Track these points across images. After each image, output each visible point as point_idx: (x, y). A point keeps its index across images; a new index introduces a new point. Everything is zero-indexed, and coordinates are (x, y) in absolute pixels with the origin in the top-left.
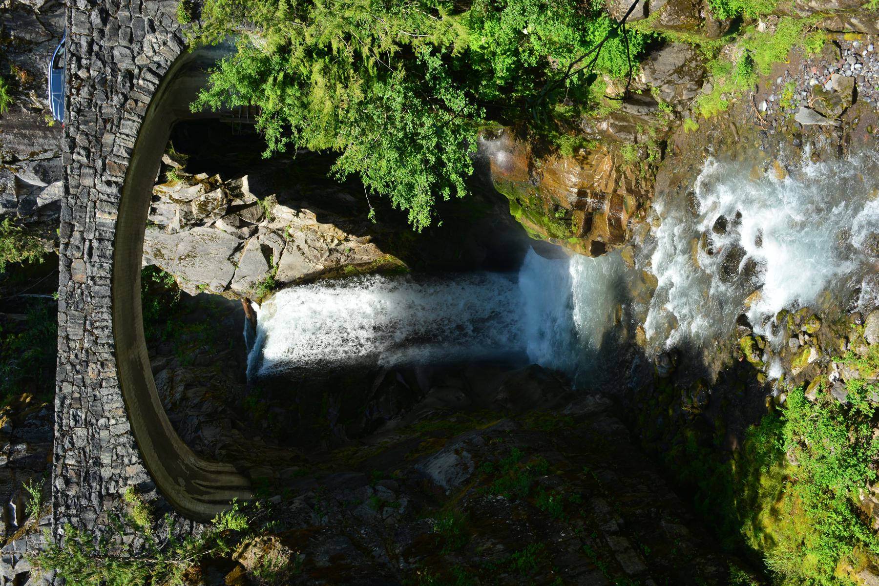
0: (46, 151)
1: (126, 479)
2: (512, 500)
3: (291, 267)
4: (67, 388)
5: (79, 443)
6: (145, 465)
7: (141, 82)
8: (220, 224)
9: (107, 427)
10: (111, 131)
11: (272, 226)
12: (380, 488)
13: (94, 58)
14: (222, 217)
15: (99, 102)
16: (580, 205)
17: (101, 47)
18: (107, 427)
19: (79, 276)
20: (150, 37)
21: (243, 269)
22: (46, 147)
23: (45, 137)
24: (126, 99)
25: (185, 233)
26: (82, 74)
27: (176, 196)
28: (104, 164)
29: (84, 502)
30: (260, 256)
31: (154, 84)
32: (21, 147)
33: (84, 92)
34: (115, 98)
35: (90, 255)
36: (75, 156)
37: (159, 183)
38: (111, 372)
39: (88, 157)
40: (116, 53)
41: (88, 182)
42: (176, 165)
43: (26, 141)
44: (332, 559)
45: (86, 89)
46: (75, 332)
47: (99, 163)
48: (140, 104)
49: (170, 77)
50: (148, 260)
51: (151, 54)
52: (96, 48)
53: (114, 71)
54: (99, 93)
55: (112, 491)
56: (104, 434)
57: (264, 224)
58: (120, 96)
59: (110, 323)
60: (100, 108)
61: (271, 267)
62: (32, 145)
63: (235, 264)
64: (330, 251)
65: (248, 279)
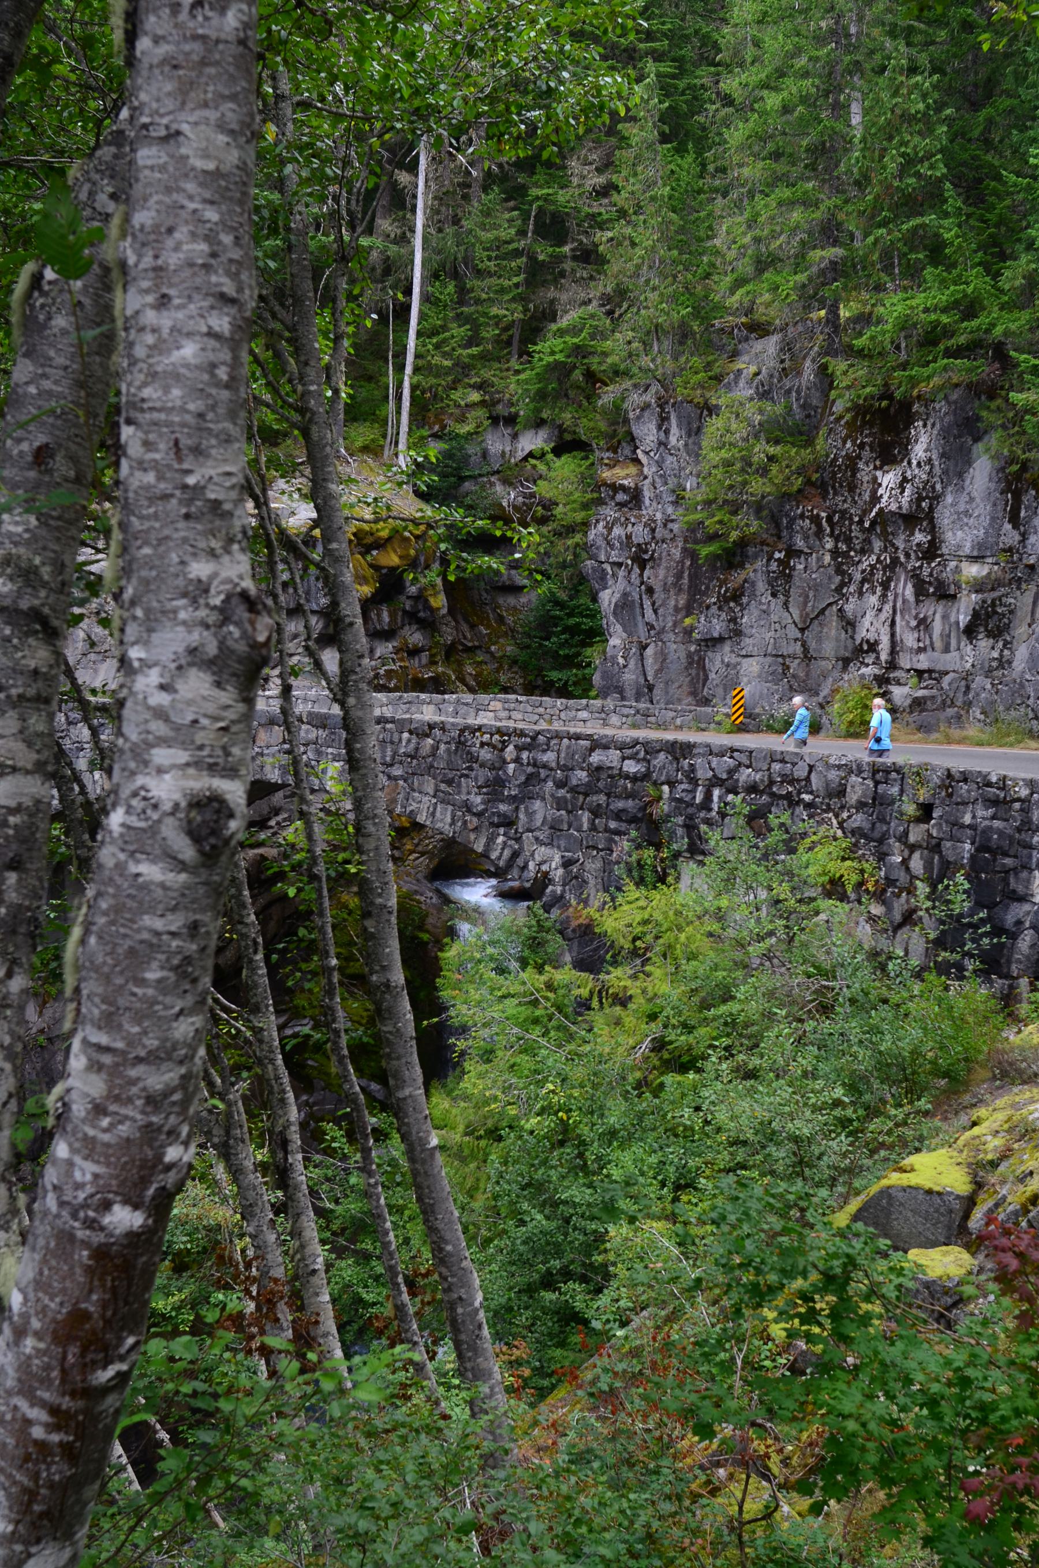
0: (655, 611)
7: (500, 839)
10: (437, 791)
13: (530, 770)
15: (473, 774)
17: (545, 781)
20: (557, 860)
22: (661, 611)
24: (479, 815)
26: (510, 752)
28: (396, 779)
31: (499, 858)
32: (662, 572)
34: (478, 799)
36: (406, 735)
39: (407, 755)
40: (537, 805)
43: (670, 580)
45: (489, 756)
47: (397, 771)
48: (472, 836)
51: (538, 858)
52: (543, 773)
53: (513, 799)
54: (483, 775)
58: (481, 808)
60: (467, 776)
62: (666, 589)
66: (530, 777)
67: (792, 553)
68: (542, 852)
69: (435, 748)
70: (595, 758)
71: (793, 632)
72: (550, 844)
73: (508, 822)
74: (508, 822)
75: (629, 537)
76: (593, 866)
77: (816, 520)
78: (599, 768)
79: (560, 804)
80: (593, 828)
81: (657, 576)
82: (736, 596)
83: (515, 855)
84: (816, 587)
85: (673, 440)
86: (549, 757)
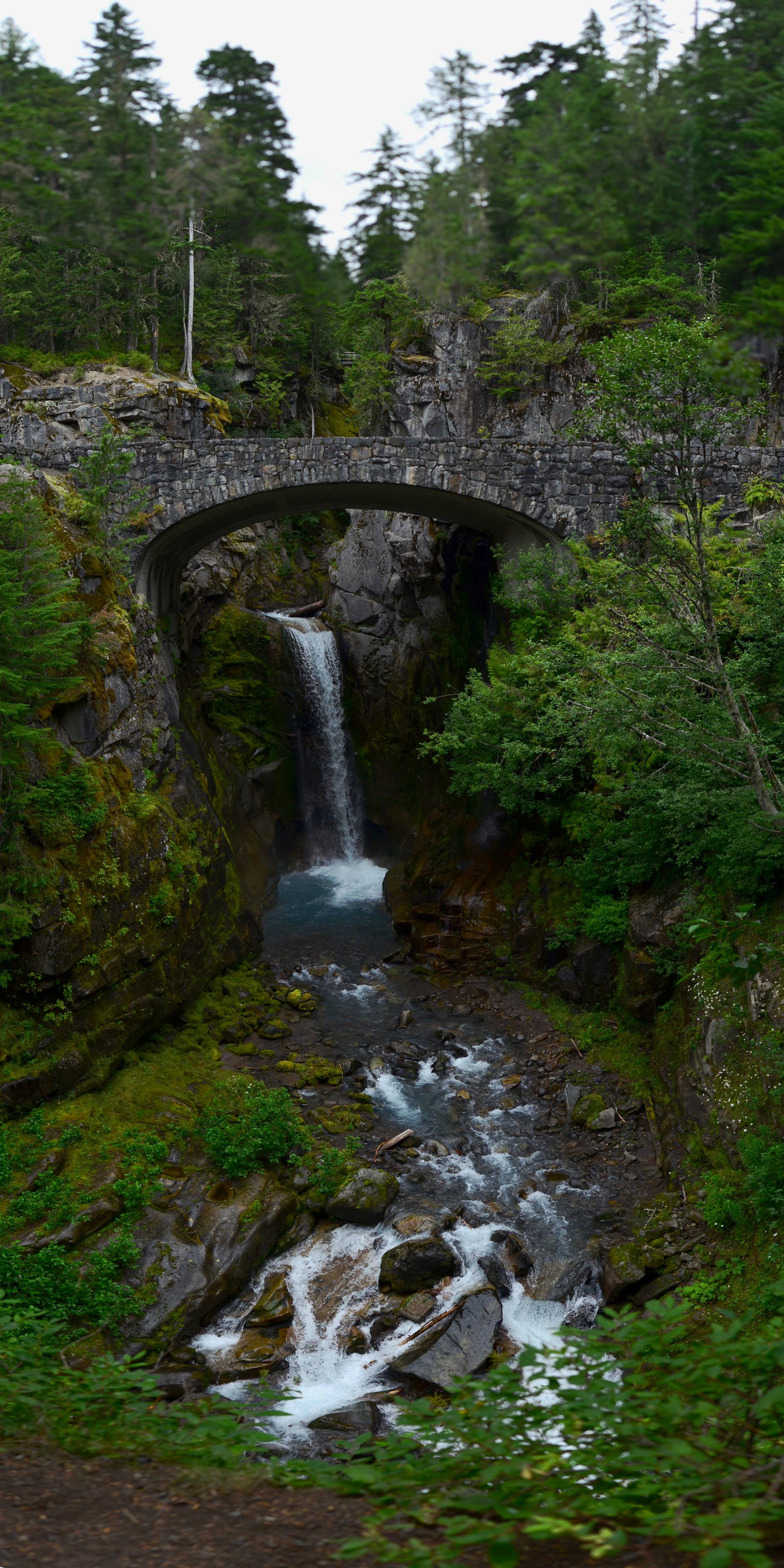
1: (171, 503)
2: (164, 859)
3: (358, 643)
4: (252, 448)
5: (203, 461)
6: (184, 519)
8: (396, 578)
9: (218, 483)
11: (396, 624)
12: (168, 734)
14: (402, 579)
16: (445, 909)
18: (218, 483)
19: (356, 454)
20: (572, 510)
21: (354, 600)
23: (467, 426)
24: (517, 490)
25: (386, 547)
27: (420, 537)
28: (458, 473)
29: (150, 468)
30: (367, 615)
33: (520, 456)
35: (375, 463)
37: (432, 521)
38: (268, 485)
41: (442, 459)
42: (449, 537)
44: (111, 691)
46: (305, 451)
47: (459, 469)
49: (538, 528)
50: (357, 515)
52: (560, 465)
54: (520, 468)
55: (160, 491)
56: (211, 481)
57: (398, 617)
59: (314, 481)
61: (358, 624)
62: (460, 415)
63: (358, 593)
64: (376, 679)
65: (344, 606)
66: (552, 467)
67: (553, 393)
68: (560, 508)
69: (485, 455)
70: (597, 454)
71: (551, 433)
72: (567, 503)
73: (538, 493)
74: (538, 493)
75: (436, 388)
76: (597, 512)
77: (567, 378)
78: (600, 460)
79: (573, 481)
80: (596, 492)
81: (455, 408)
82: (521, 414)
83: (544, 511)
84: (564, 411)
85: (459, 341)
86: (565, 456)
